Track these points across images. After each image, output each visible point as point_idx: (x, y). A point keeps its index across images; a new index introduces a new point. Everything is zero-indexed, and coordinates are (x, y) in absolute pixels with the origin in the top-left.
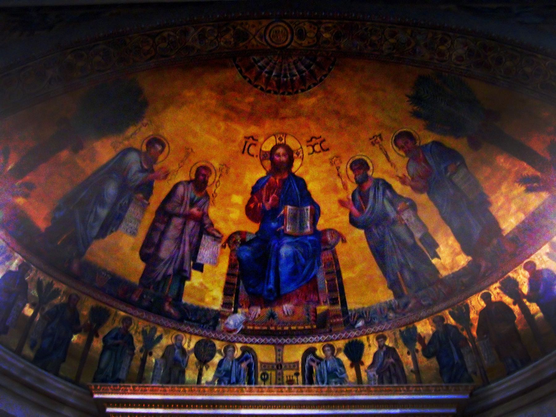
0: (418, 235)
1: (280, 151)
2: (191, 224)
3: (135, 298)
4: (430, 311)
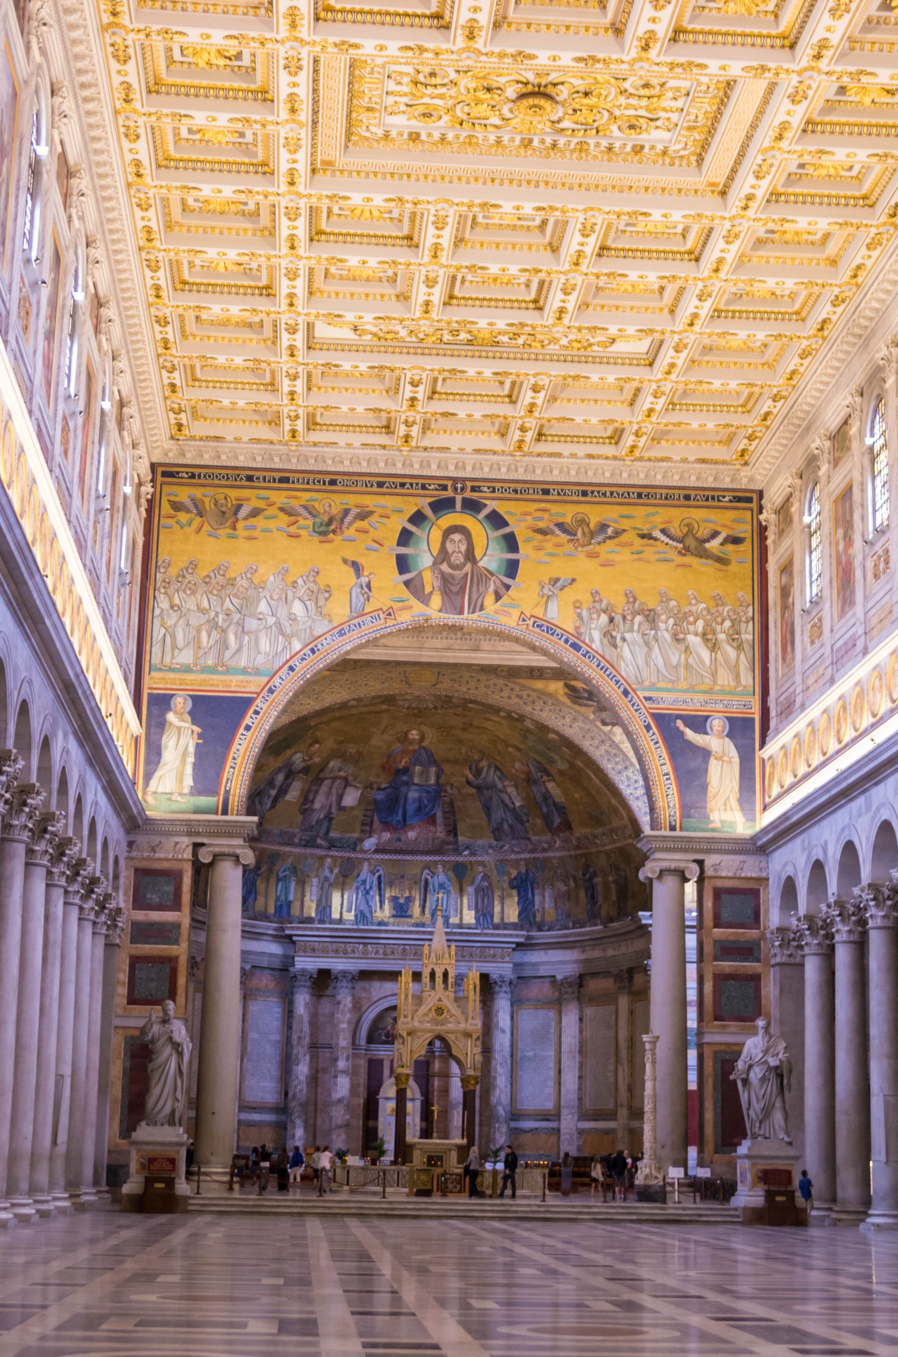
0: (518, 804)
1: (414, 732)
2: (338, 781)
4: (518, 856)
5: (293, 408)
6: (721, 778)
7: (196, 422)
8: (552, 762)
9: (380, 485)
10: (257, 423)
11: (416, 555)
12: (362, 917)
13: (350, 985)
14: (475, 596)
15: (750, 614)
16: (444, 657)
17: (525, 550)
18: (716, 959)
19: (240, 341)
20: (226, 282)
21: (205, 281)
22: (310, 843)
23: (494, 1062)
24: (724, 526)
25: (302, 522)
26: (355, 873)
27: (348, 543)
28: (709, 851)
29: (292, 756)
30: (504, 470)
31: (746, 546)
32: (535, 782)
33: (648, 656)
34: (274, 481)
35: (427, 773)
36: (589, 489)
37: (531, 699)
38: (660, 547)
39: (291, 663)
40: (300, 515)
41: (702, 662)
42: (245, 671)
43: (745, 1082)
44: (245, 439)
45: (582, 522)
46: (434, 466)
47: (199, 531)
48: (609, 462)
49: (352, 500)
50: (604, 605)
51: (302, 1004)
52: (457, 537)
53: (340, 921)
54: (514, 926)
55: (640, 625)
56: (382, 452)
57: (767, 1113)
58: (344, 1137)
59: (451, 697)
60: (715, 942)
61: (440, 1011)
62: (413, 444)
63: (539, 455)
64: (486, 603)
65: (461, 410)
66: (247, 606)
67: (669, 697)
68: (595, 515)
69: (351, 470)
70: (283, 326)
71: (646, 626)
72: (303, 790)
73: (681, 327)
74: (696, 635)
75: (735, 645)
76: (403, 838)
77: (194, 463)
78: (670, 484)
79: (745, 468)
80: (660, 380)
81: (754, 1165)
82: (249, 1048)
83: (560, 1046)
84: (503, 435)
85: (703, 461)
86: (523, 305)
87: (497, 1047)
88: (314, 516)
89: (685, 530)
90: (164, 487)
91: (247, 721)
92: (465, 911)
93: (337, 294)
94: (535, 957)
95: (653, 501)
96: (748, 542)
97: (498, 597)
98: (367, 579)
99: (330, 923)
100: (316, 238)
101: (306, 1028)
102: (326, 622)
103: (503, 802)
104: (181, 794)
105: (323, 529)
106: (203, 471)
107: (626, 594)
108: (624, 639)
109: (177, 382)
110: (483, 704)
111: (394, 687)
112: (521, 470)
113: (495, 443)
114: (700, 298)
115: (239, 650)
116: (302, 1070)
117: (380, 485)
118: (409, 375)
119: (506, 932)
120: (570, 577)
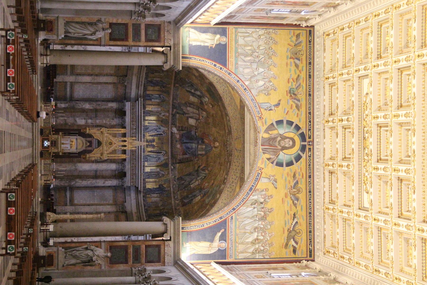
0: (192, 186)
1: (218, 144)
2: (198, 116)
3: (175, 101)
4: (171, 187)
5: (337, 76)
6: (202, 247)
7: (330, 41)
8: (208, 197)
9: (310, 113)
10: (331, 64)
11: (283, 127)
12: (146, 128)
13: (120, 123)
14: (268, 150)
15: (266, 257)
16: (247, 152)
17: (287, 169)
18: (133, 246)
19: (360, 51)
20: (382, 41)
21: (382, 33)
22: (174, 107)
23: (92, 180)
24: (300, 247)
25: (294, 84)
26: (163, 125)
27: (287, 102)
28: (174, 242)
29: (207, 97)
30: (317, 160)
31: (293, 255)
32: (200, 192)
33: (248, 218)
34: (309, 73)
35: (203, 151)
36: (312, 194)
37: (232, 187)
38: (291, 222)
39: (240, 81)
40: (297, 83)
41: (247, 239)
42: (237, 64)
43: (87, 249)
44: (325, 61)
45: (299, 191)
46: (317, 133)
47: (289, 45)
48: (322, 200)
49: (303, 102)
50: (267, 200)
51: (112, 105)
52: (291, 143)
53: (145, 120)
54: (145, 187)
55: (260, 214)
56: (322, 113)
57: (75, 257)
58: (62, 123)
59: (231, 155)
60: (140, 246)
61: (111, 144)
62: (326, 125)
63: (324, 173)
64: (266, 155)
65: (339, 140)
66: (261, 64)
67: (233, 226)
68: (302, 196)
69: (315, 102)
70: (367, 65)
71: (260, 217)
72: (194, 102)
73: (374, 216)
74: (257, 236)
75: (254, 251)
76: (177, 143)
77: (315, 42)
78: (315, 225)
79: (323, 254)
80: (354, 213)
81: (55, 252)
82: (95, 85)
83: (99, 205)
84: (331, 159)
85: (325, 237)
86: (379, 155)
87: (98, 181)
88: (296, 88)
89: (298, 231)
90: (305, 31)
91: (218, 65)
92: (150, 168)
93: (380, 84)
94: (133, 195)
95: (308, 218)
96: (294, 256)
97: (268, 159)
98: (273, 109)
99: (144, 116)
100: (400, 71)
101: (103, 107)
102: (256, 94)
103: (192, 180)
104: (189, 41)
105: (292, 92)
106: (312, 46)
107: (272, 209)
108: (254, 208)
109: (345, 30)
110: (229, 168)
111: (235, 134)
112: (317, 167)
113: (328, 156)
114: (385, 221)
115: (244, 61)
116: (87, 106)
117: (310, 113)
118: (351, 117)
119: (142, 183)
120: (277, 187)
